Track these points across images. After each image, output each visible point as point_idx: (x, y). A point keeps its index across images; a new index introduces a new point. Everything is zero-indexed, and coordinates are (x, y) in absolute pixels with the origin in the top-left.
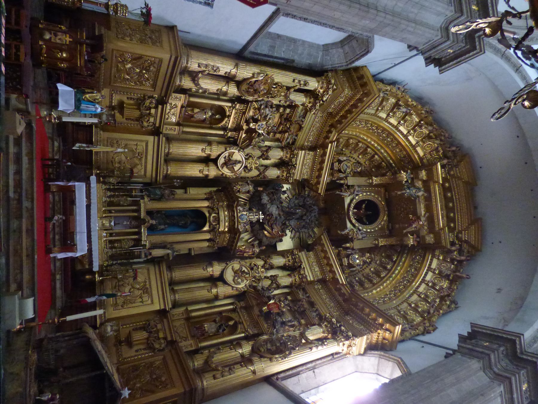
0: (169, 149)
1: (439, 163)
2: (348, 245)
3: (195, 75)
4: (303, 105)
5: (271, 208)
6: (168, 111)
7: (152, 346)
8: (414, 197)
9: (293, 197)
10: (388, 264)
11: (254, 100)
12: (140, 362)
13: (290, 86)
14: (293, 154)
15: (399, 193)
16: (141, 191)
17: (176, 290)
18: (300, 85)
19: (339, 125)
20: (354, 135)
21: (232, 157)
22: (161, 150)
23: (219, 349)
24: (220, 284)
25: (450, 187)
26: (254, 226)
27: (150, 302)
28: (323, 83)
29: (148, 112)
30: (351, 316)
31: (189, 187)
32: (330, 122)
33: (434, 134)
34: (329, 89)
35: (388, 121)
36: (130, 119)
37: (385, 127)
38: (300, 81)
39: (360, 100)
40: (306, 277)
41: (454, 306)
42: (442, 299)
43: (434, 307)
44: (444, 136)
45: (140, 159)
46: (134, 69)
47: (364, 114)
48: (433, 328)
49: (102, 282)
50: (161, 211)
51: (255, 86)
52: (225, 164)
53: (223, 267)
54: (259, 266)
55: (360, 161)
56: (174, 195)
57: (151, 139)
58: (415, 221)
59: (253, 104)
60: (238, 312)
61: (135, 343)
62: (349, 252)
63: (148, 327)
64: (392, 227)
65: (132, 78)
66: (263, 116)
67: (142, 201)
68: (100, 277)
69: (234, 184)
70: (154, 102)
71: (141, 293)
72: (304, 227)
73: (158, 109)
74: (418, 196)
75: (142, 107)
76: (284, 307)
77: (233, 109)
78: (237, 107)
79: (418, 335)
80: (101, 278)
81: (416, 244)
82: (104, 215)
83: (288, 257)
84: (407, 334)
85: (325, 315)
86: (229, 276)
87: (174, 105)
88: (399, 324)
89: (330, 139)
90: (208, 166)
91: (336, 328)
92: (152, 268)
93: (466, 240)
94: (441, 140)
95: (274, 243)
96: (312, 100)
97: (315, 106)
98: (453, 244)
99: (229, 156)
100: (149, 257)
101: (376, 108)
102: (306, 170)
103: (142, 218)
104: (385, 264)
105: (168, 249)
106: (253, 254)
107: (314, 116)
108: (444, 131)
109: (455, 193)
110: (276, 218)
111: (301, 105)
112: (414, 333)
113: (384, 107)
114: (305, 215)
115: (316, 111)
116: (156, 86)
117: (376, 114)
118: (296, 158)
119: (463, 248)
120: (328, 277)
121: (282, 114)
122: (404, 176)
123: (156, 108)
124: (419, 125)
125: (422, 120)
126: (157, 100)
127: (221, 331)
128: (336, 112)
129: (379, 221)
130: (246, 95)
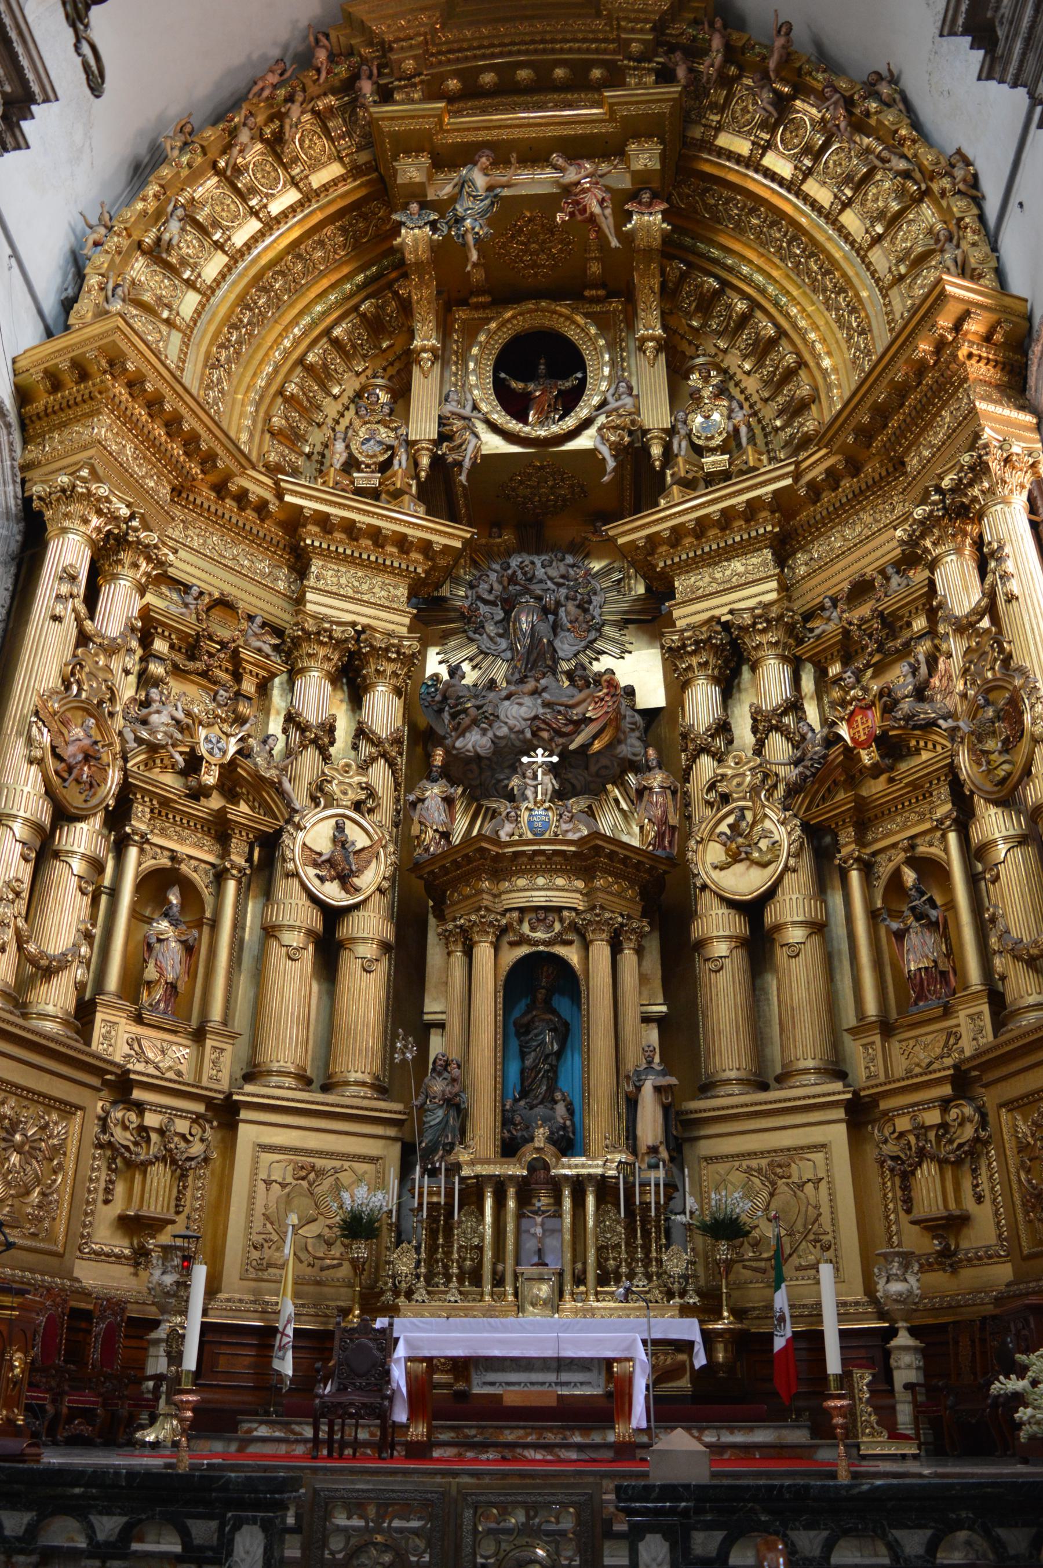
0: (288, 1074)
1: (372, 110)
2: (656, 451)
3: (30, 969)
4: (142, 591)
5: (511, 722)
6: (151, 1070)
7: (966, 1148)
8: (492, 204)
9: (472, 640)
10: (729, 307)
11: (120, 762)
12: (1015, 1186)
13: (74, 632)
14: (318, 633)
15: (474, 256)
17: (783, 1067)
18: (72, 596)
19: (220, 464)
20: (257, 411)
21: (320, 854)
22: (288, 1100)
23: (993, 920)
24: (770, 917)
25: (457, 74)
26: (573, 786)
27: (818, 1157)
28: (67, 516)
29: (154, 1137)
30: (908, 450)
31: (422, 1013)
32: (206, 496)
33: (266, 125)
34: (89, 493)
35: (210, 287)
36: (178, 1199)
37: (233, 296)
38: (59, 597)
39: (135, 384)
40: (766, 606)
41: (884, 83)
42: (860, 126)
43: (885, 154)
44: (275, 87)
45: (321, 1173)
46: (9, 1171)
47: (182, 370)
48: (960, 165)
49: (738, 1313)
50: (503, 1111)
51: (74, 756)
52: (344, 879)
53: (715, 902)
54: (717, 775)
55: (350, 393)
56: (447, 1063)
57: (247, 1134)
58: (577, 203)
59: (135, 769)
60: (874, 854)
61: (952, 1206)
63: (903, 1163)
64: (596, 287)
65: (38, 1181)
66: (179, 736)
67: (464, 1173)
68: (721, 1317)
69: (419, 851)
70: (119, 1115)
71: (787, 1184)
72: (583, 607)
73: (148, 1103)
74: (490, 188)
75: (137, 1154)
76: (866, 690)
77: (147, 841)
78: (143, 827)
79: (981, 218)
80: (726, 1314)
81: (664, 206)
82: (510, 1298)
83: (690, 668)
84: (975, 256)
85: (902, 542)
87: (132, 1049)
88: (939, 281)
89: (268, 496)
90: (353, 940)
91: (944, 508)
92: (706, 1148)
93: (653, 29)
94: (290, 99)
96: (127, 557)
97: (147, 546)
98: (665, 76)
99: (316, 865)
100: (664, 1154)
101: (164, 328)
102: (376, 590)
103: (525, 1173)
104: (730, 317)
105: (639, 1089)
106: (674, 793)
107: (182, 553)
108: (256, 89)
109: (484, 57)
110: (546, 705)
111: (142, 596)
112: (974, 232)
113: (159, 298)
114: (539, 599)
115: (165, 544)
116: (66, 1103)
117: (183, 327)
118: (332, 623)
119: (684, 40)
120: (769, 528)
121: (170, 668)
123: (140, 1108)
124: (229, 177)
126: (114, 1103)
127: (934, 914)
128: (170, 472)
129: (572, 333)
130: (103, 791)
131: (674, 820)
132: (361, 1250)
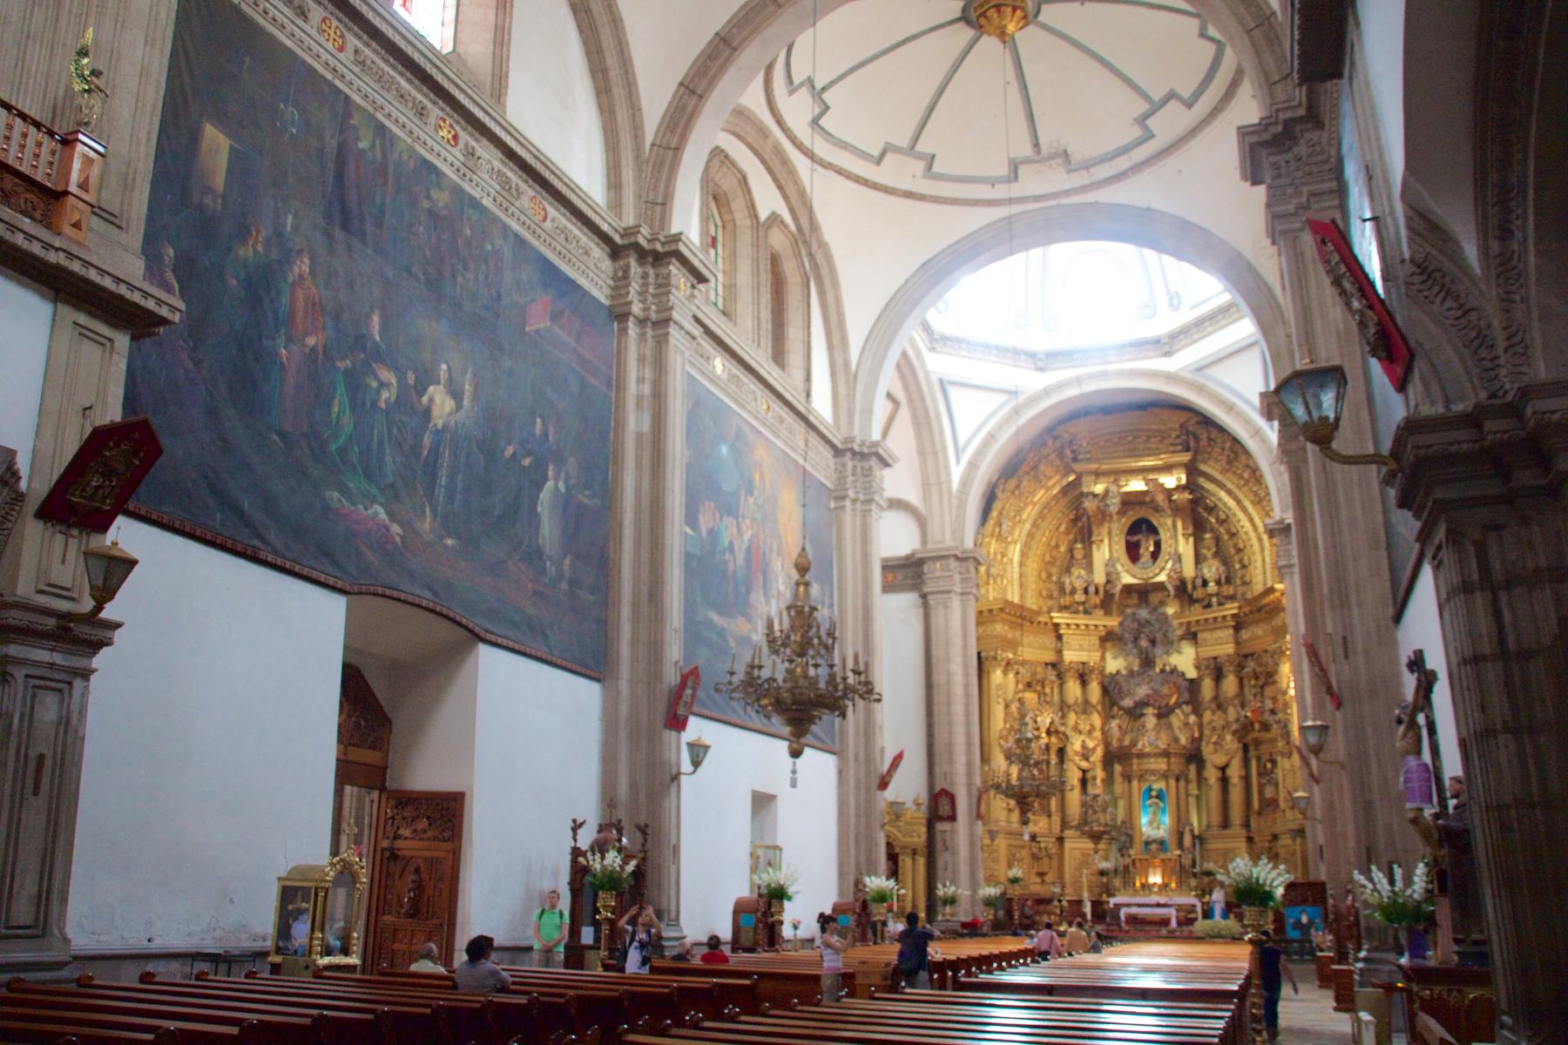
16: (1122, 855)
24: (1229, 772)
40: (1229, 656)
52: (1087, 759)
57: (1068, 845)
62: (1199, 582)
72: (1165, 635)
86: (1220, 759)
89: (1048, 620)
94: (1040, 460)
95: (1187, 683)
110: (1152, 689)
122: (1089, 504)
125: (1013, 493)
131: (1196, 735)
132: (1105, 880)
